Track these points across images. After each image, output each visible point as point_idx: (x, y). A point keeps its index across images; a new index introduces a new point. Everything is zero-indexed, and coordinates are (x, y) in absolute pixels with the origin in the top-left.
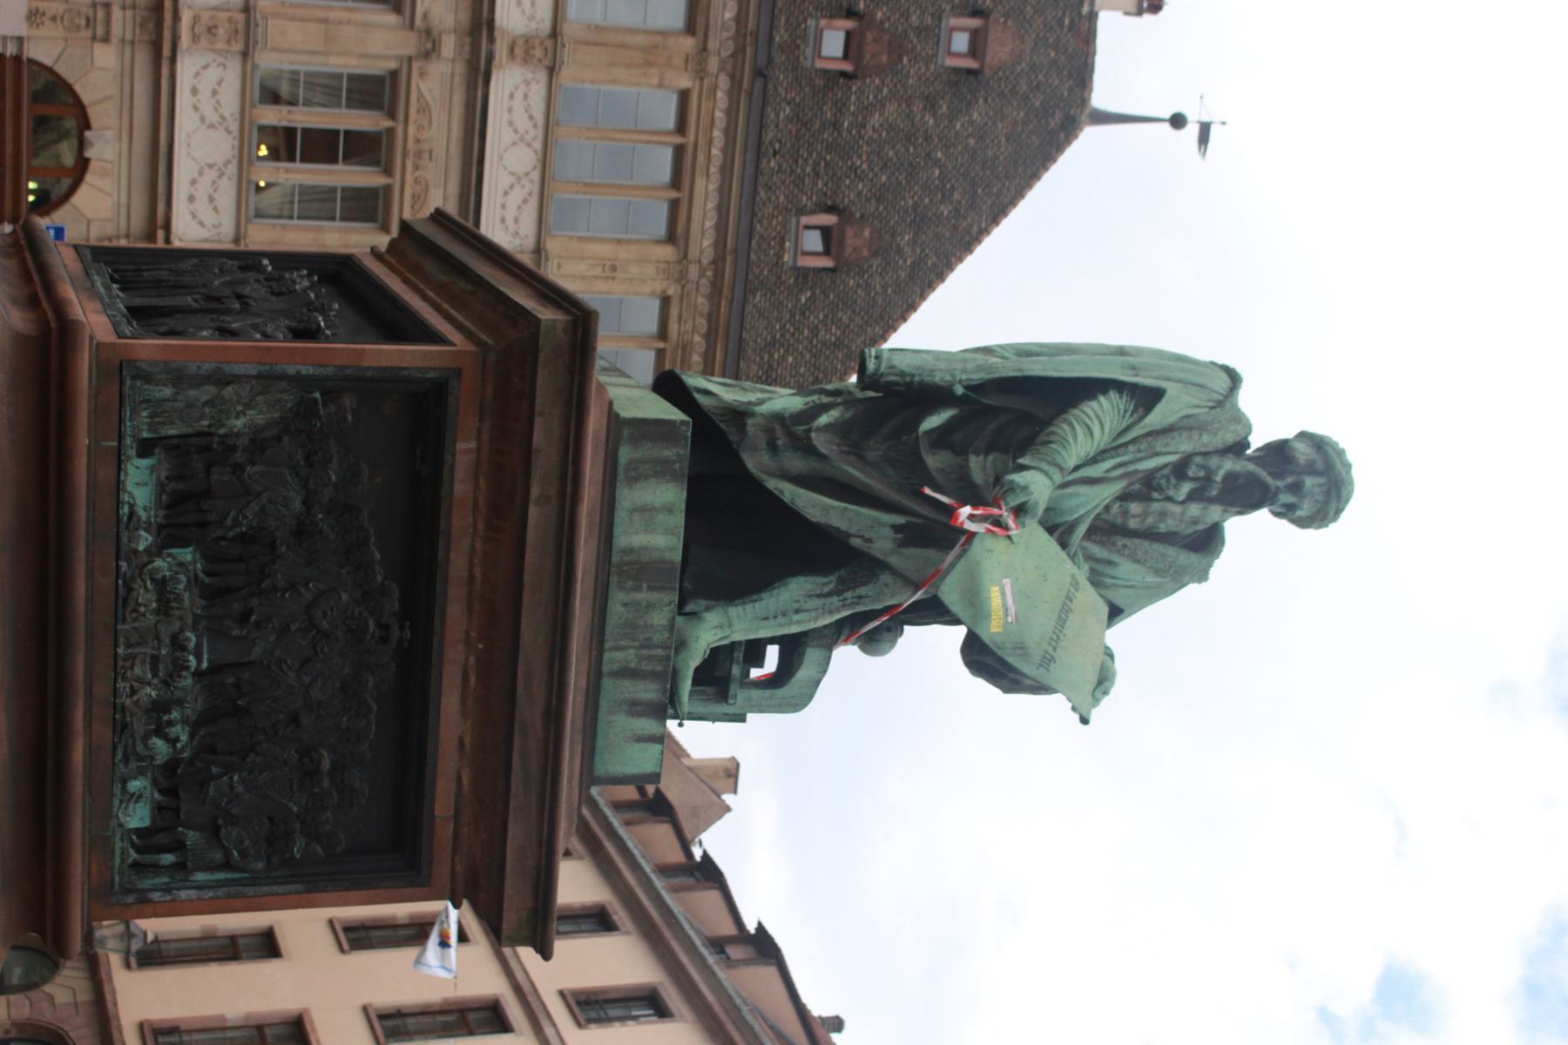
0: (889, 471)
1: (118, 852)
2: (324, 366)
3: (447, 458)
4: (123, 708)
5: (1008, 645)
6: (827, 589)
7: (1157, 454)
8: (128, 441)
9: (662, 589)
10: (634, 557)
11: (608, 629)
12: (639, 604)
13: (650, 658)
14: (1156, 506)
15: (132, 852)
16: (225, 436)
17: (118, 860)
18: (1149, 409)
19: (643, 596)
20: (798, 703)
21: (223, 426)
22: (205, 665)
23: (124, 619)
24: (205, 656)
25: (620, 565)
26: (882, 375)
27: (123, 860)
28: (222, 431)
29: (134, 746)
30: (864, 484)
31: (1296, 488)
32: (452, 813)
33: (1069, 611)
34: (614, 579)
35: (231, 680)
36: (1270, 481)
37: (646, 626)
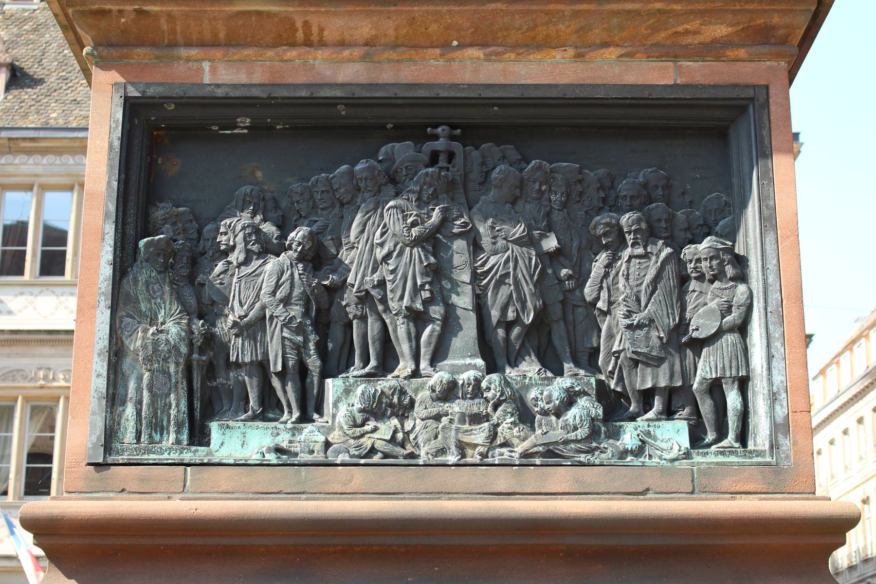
1: (721, 459)
2: (103, 234)
3: (220, 92)
4: (525, 455)
8: (187, 457)
15: (724, 443)
16: (191, 345)
17: (733, 459)
21: (176, 348)
22: (480, 362)
23: (412, 456)
24: (468, 361)
27: (732, 453)
28: (184, 349)
29: (576, 441)
32: (670, 64)
35: (501, 332)
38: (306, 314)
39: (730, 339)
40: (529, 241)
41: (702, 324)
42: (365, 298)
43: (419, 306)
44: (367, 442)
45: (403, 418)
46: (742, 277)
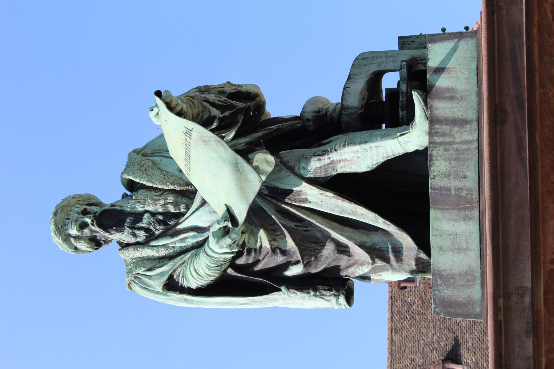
0: (319, 235)
5: (212, 142)
6: (342, 164)
7: (163, 245)
9: (441, 189)
10: (463, 213)
11: (476, 157)
12: (455, 177)
13: (444, 135)
14: (160, 210)
18: (171, 276)
19: (453, 184)
20: (362, 60)
25: (472, 208)
26: (335, 295)
30: (333, 229)
31: (83, 226)
33: (186, 160)
34: (475, 196)
36: (97, 229)
37: (449, 160)
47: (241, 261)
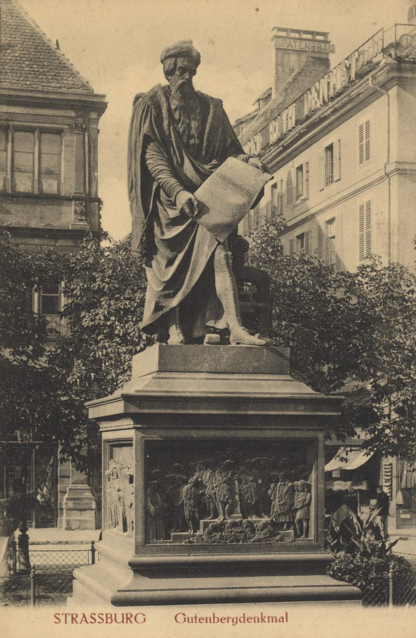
38: (195, 501)
39: (305, 508)
40: (255, 481)
41: (298, 504)
42: (210, 497)
43: (225, 500)
44: (213, 539)
45: (222, 532)
46: (309, 491)
47: (162, 193)
